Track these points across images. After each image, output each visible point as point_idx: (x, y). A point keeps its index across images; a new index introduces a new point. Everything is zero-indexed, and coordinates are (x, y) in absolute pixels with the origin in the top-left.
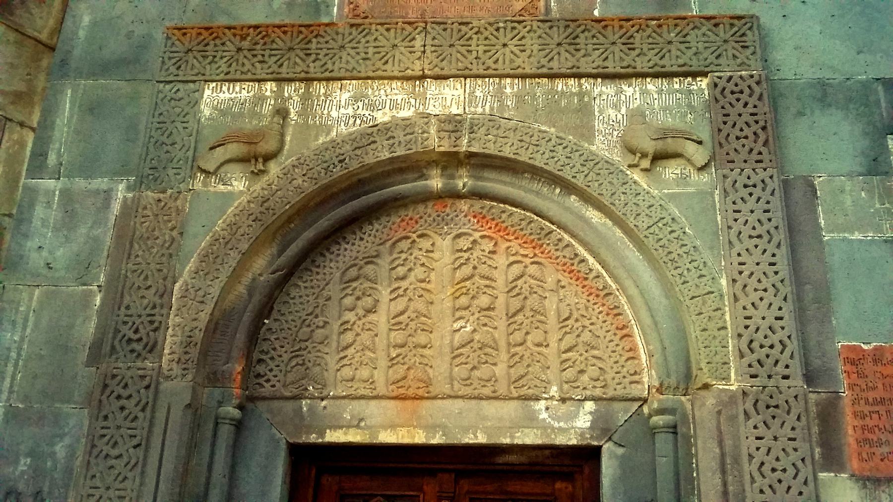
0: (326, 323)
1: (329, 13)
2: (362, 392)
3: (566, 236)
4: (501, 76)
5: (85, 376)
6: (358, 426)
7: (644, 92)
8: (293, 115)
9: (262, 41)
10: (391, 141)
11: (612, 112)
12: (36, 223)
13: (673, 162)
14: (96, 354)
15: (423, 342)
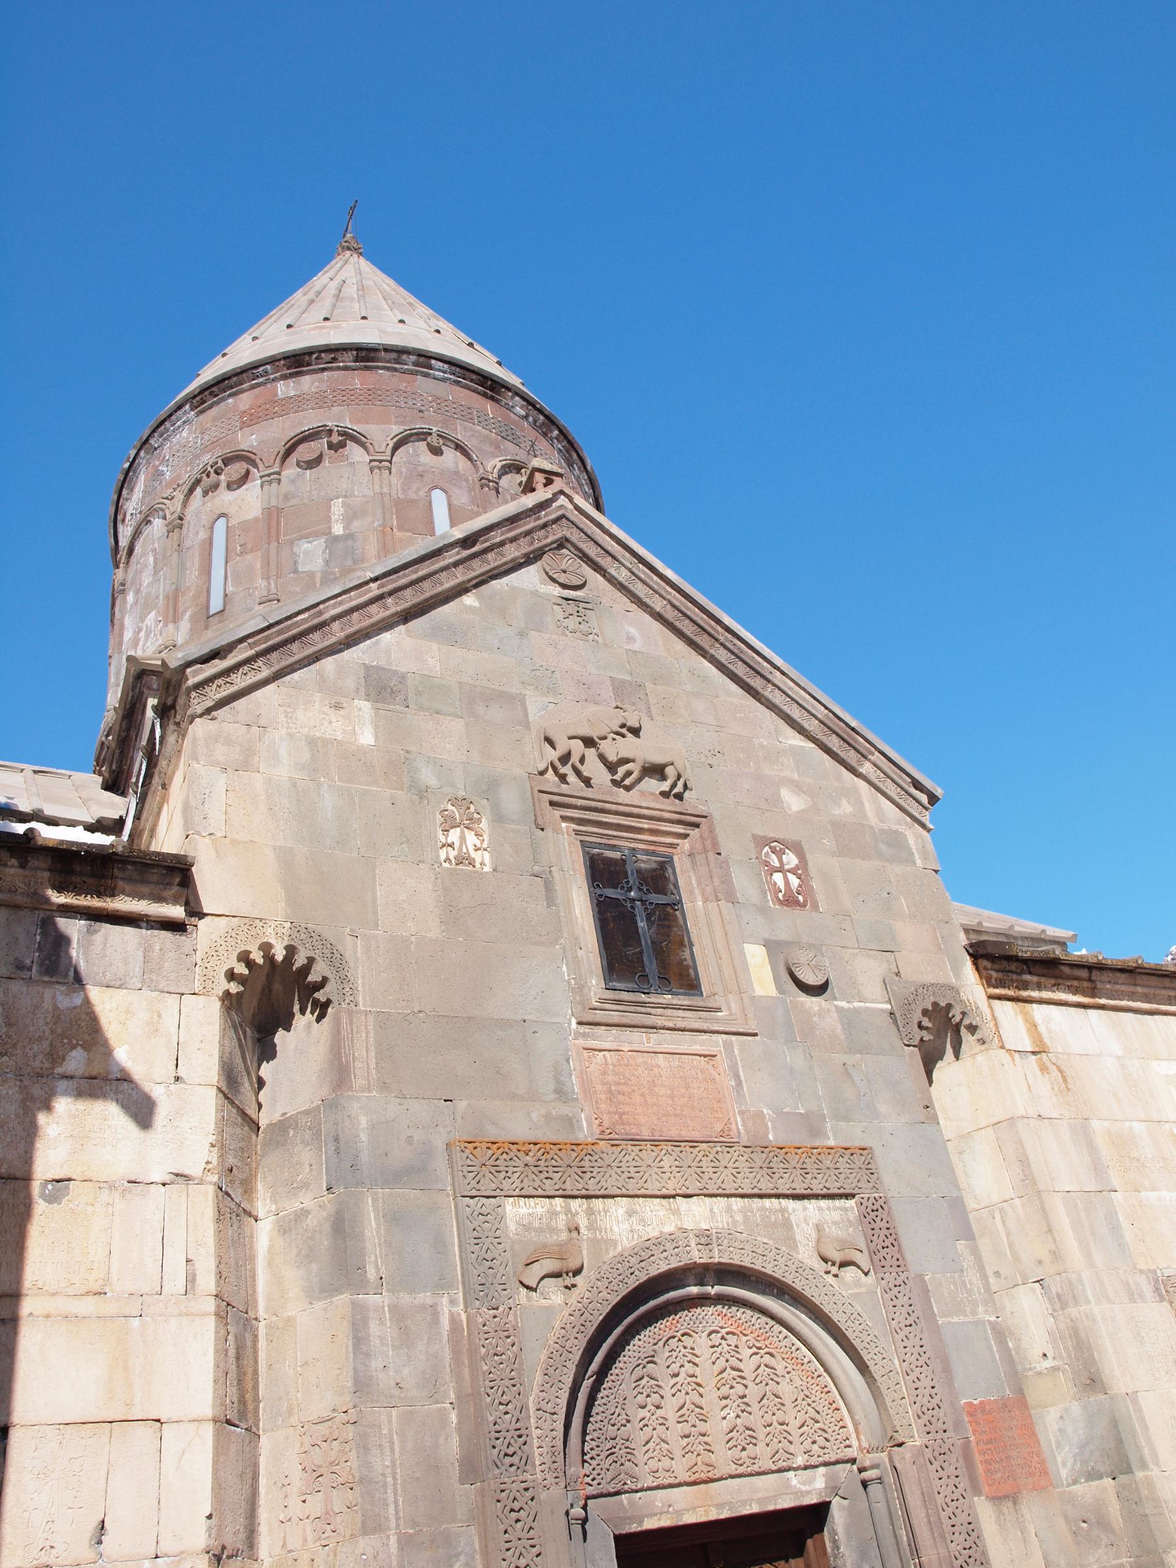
0: (628, 1421)
1: (581, 1128)
2: (666, 1482)
3: (784, 1331)
4: (728, 1196)
5: (465, 1494)
6: (667, 1512)
7: (820, 1209)
8: (582, 1230)
9: (544, 1158)
10: (665, 1254)
11: (804, 1225)
12: (375, 1341)
13: (851, 1269)
14: (470, 1470)
15: (703, 1431)
